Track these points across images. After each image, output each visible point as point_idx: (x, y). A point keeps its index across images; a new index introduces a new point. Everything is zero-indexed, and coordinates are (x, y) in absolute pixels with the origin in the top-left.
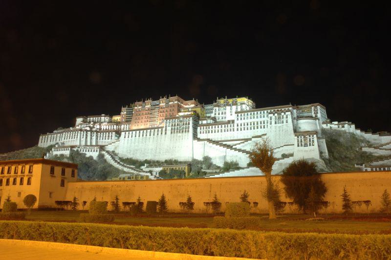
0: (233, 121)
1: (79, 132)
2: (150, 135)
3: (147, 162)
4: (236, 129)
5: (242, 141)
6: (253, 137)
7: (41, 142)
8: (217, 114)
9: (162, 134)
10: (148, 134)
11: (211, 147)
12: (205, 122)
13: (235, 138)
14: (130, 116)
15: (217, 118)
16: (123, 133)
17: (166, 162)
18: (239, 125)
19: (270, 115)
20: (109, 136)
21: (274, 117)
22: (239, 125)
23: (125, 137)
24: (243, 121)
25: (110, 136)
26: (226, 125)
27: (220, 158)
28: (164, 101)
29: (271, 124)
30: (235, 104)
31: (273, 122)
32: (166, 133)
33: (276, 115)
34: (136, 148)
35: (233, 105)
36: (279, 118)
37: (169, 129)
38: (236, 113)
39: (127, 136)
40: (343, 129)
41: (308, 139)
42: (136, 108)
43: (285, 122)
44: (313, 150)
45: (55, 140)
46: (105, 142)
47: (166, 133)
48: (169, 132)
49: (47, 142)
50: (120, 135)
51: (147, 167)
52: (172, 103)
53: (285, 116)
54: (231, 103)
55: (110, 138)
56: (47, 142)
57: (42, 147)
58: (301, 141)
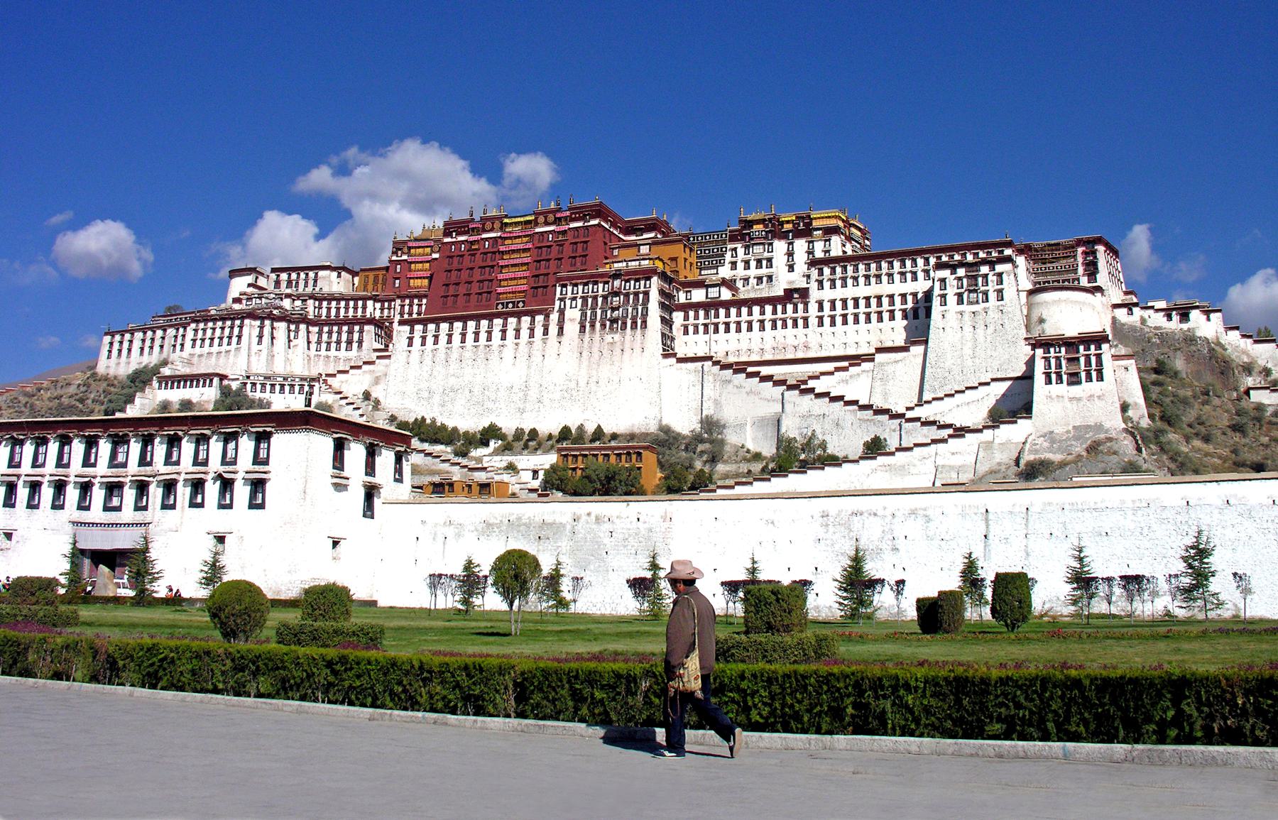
0: (804, 293)
1: (247, 321)
2: (503, 338)
3: (491, 433)
4: (813, 321)
5: (845, 364)
6: (879, 350)
7: (109, 357)
8: (740, 265)
9: (546, 332)
10: (496, 334)
11: (730, 382)
12: (698, 295)
13: (812, 354)
15: (739, 284)
16: (401, 332)
18: (827, 306)
20: (349, 342)
22: (827, 306)
23: (410, 344)
24: (839, 293)
25: (356, 336)
26: (779, 308)
27: (761, 423)
28: (551, 218)
29: (944, 303)
30: (804, 230)
31: (952, 299)
32: (561, 331)
33: (961, 272)
34: (452, 381)
35: (799, 234)
36: (973, 278)
37: (573, 314)
38: (813, 263)
40: (1185, 326)
41: (1082, 360)
43: (992, 296)
44: (1099, 397)
45: (157, 348)
46: (337, 359)
47: (561, 331)
48: (572, 328)
50: (389, 336)
51: (497, 452)
52: (580, 224)
53: (992, 278)
54: (788, 227)
55: (355, 345)
57: (112, 372)
58: (1059, 366)
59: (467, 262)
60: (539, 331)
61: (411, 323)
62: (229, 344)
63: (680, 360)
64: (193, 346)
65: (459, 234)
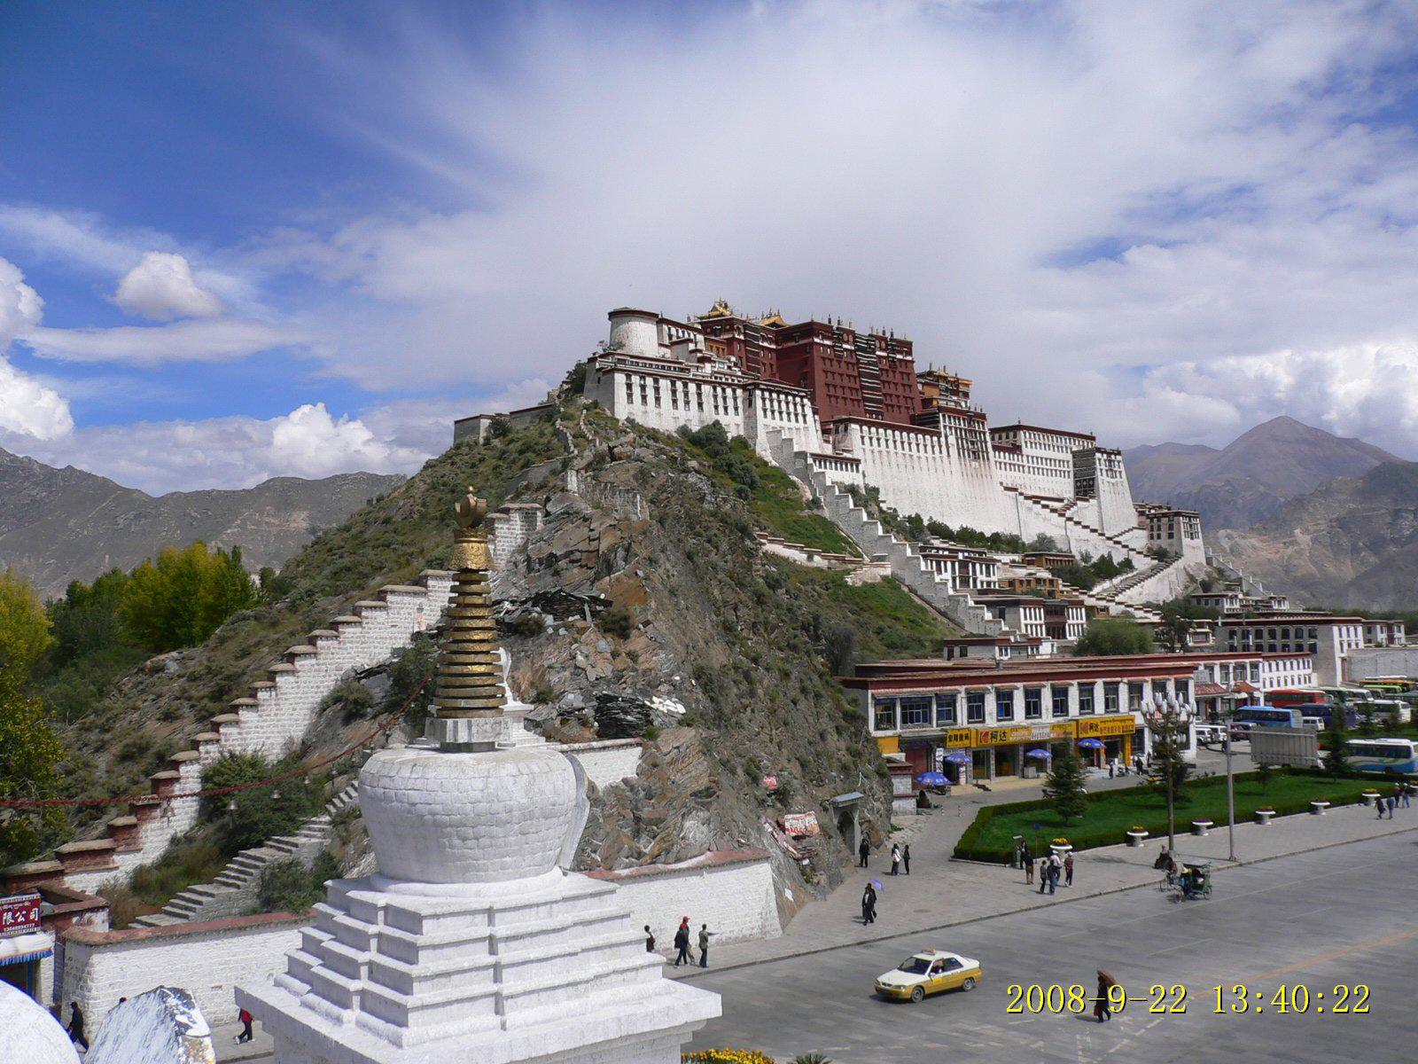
0: (1019, 448)
4: (1026, 469)
7: (630, 396)
9: (941, 452)
11: (1030, 509)
14: (758, 354)
17: (996, 537)
19: (1098, 455)
21: (1102, 461)
23: (863, 443)
28: (883, 345)
33: (1105, 455)
36: (1110, 461)
37: (952, 439)
39: (867, 440)
42: (816, 340)
48: (954, 451)
49: (658, 399)
56: (658, 399)
59: (835, 367)
60: (937, 449)
61: (861, 423)
62: (797, 421)
63: (1007, 489)
64: (765, 416)
65: (824, 337)
